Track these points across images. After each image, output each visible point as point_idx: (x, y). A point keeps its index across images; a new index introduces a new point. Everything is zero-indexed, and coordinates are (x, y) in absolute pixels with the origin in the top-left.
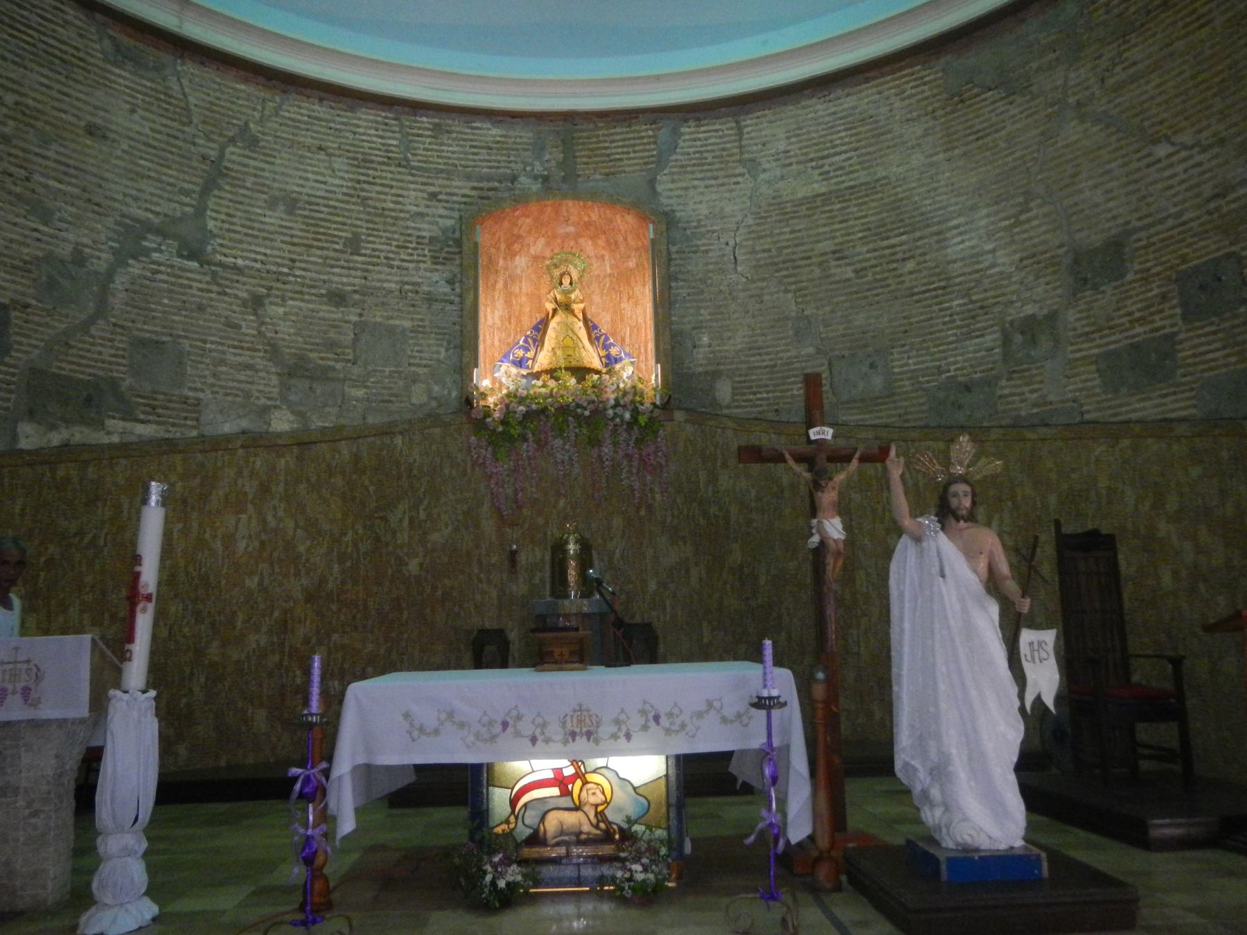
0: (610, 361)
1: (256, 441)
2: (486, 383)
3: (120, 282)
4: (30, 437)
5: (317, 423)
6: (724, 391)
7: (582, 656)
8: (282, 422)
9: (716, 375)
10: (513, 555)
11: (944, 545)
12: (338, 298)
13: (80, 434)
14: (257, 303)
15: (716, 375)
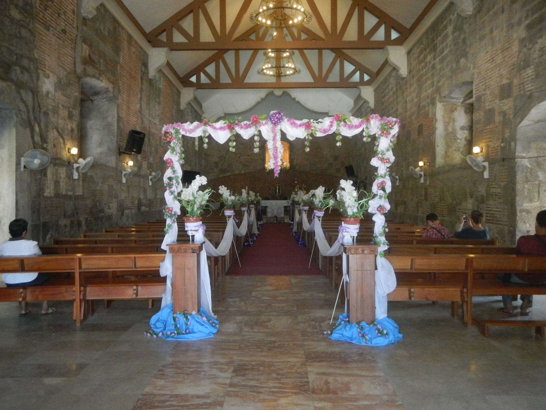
0: (283, 163)
1: (240, 174)
2: (267, 166)
3: (227, 157)
4: (221, 176)
5: (246, 172)
6: (297, 167)
7: (277, 199)
8: (243, 172)
9: (297, 165)
10: (270, 188)
11: (302, 192)
12: (248, 155)
13: (224, 175)
14: (239, 157)
15: (297, 165)
